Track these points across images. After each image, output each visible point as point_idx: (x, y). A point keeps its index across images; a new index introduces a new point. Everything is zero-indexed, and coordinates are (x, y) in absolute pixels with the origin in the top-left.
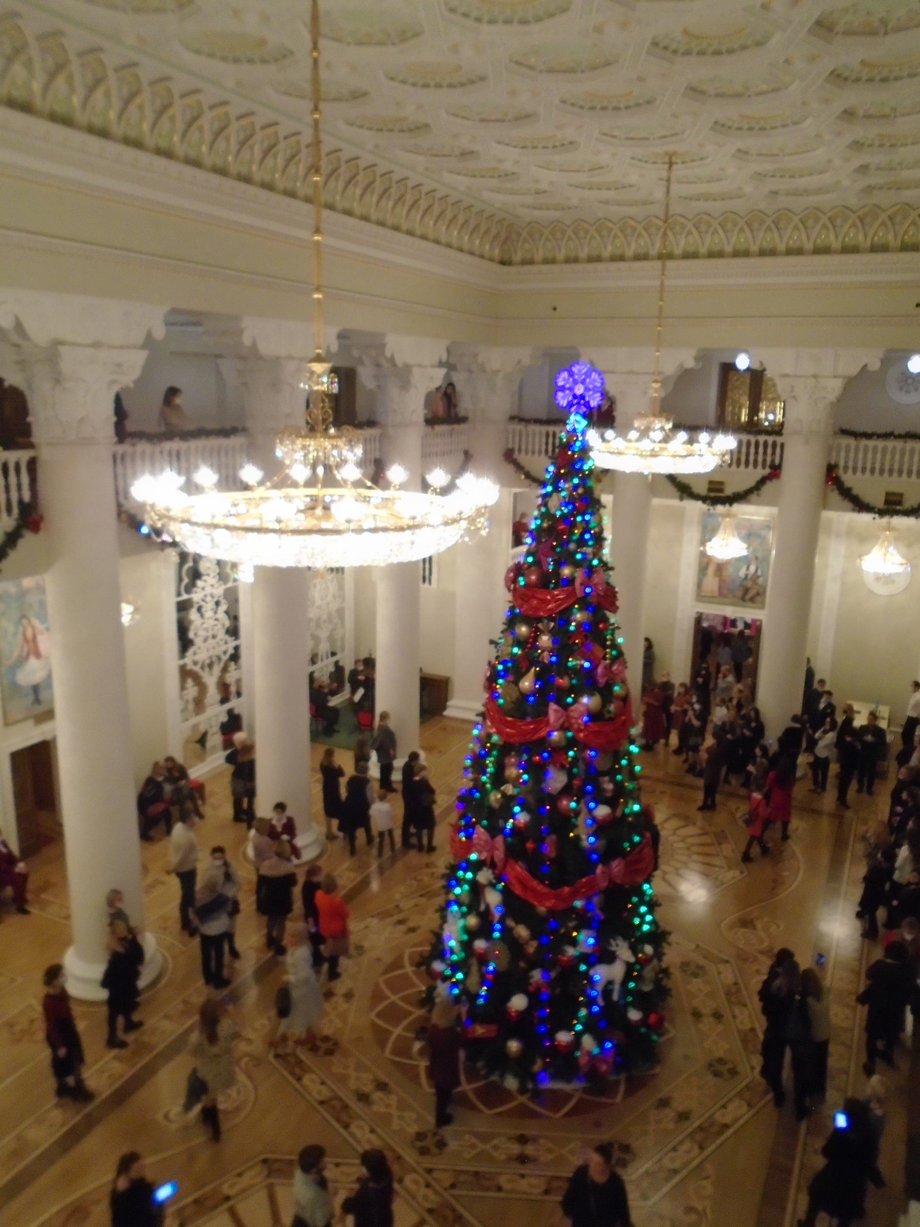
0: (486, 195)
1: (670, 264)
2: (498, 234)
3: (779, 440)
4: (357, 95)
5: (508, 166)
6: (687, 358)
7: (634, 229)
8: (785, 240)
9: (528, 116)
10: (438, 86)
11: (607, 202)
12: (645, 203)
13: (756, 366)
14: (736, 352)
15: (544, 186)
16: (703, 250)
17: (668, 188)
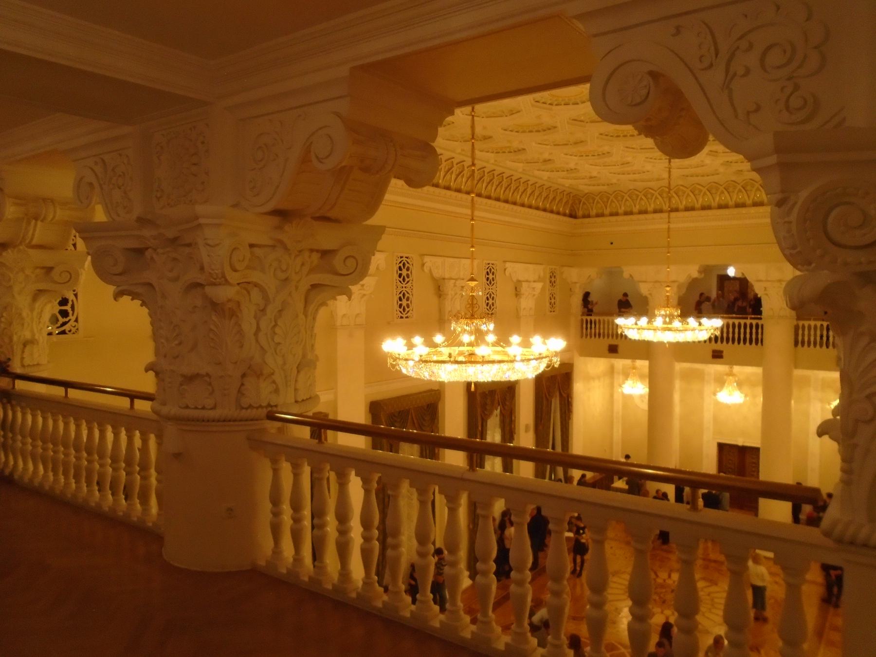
0: (560, 181)
1: (673, 215)
2: (567, 202)
3: (760, 322)
4: (486, 138)
5: (572, 165)
6: (693, 271)
7: (653, 195)
8: (752, 197)
9: (582, 142)
10: (531, 131)
11: (635, 181)
12: (658, 180)
13: (739, 276)
14: (726, 267)
15: (594, 174)
16: (697, 206)
17: (670, 172)
